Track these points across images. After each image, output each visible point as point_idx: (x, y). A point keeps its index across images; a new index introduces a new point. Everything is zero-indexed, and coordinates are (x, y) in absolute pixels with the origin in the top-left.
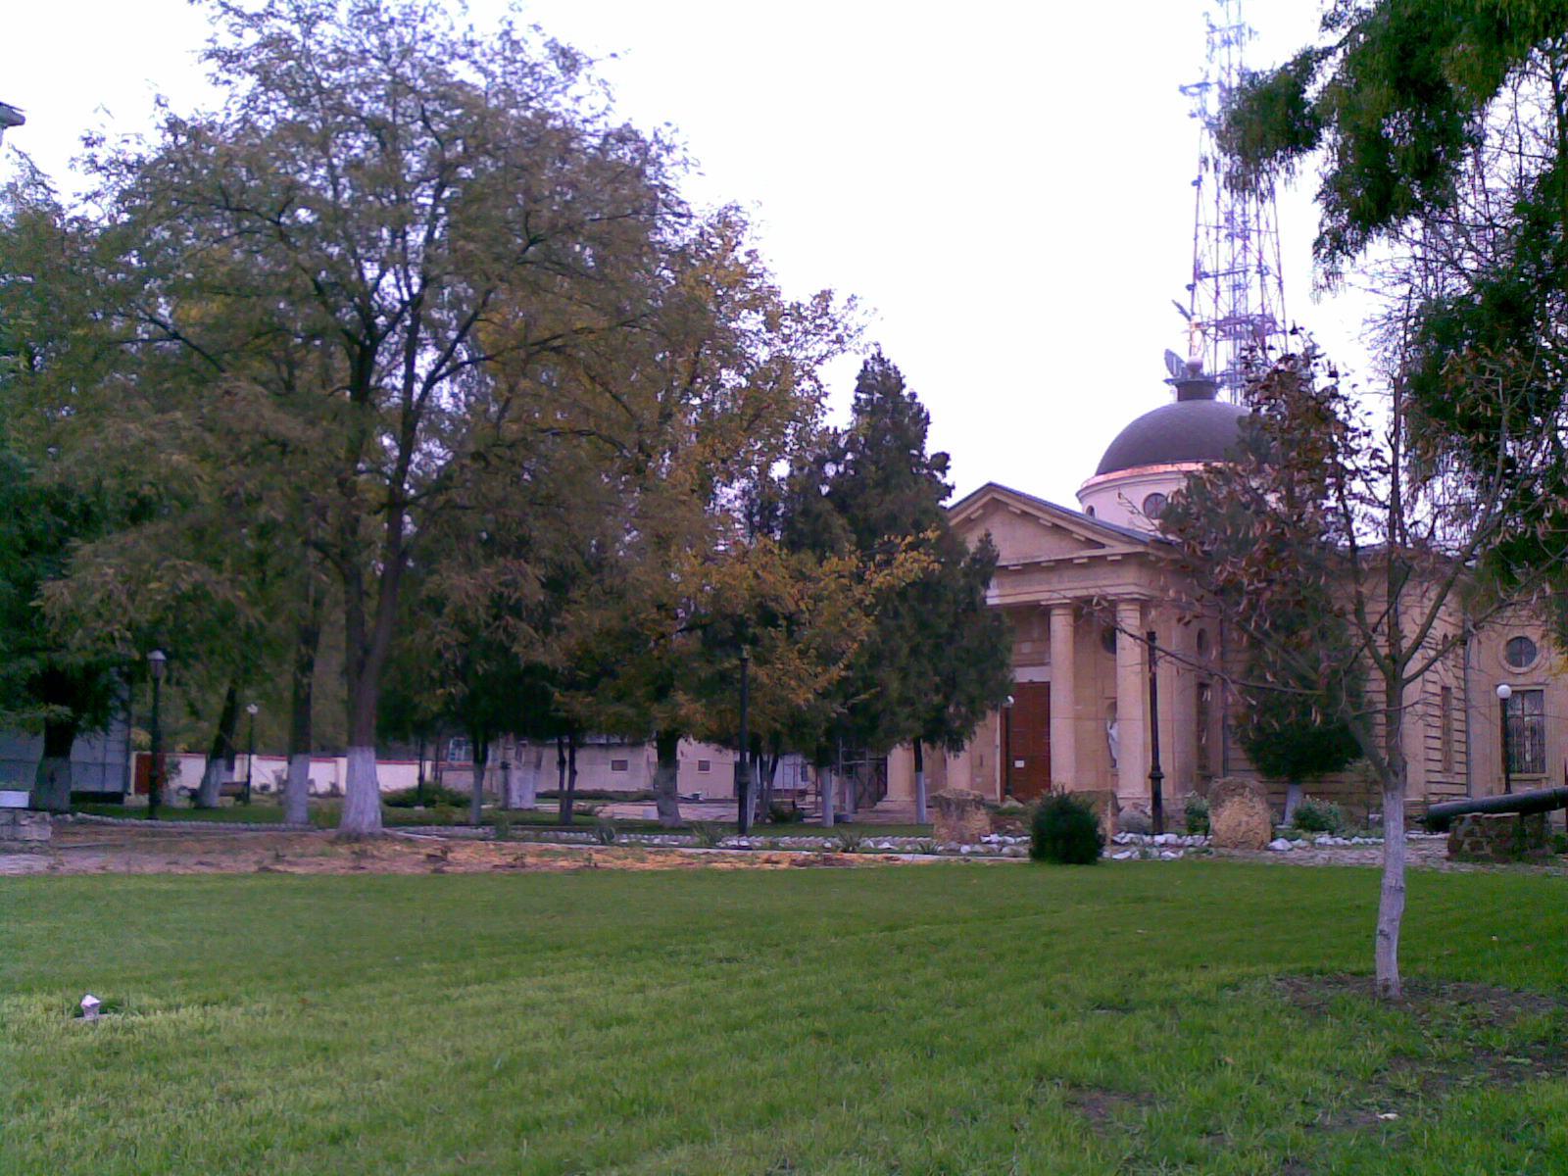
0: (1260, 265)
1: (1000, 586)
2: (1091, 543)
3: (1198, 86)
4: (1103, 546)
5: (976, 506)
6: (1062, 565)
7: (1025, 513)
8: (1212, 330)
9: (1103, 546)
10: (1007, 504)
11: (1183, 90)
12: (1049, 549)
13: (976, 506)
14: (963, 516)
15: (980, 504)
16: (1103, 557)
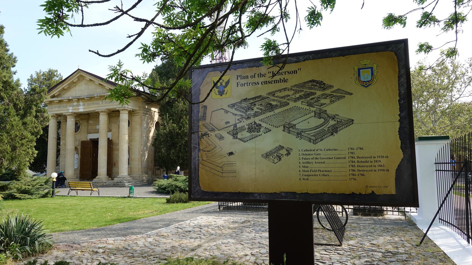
1: (84, 105)
5: (75, 78)
7: (91, 80)
13: (75, 78)
14: (71, 81)
15: (76, 77)
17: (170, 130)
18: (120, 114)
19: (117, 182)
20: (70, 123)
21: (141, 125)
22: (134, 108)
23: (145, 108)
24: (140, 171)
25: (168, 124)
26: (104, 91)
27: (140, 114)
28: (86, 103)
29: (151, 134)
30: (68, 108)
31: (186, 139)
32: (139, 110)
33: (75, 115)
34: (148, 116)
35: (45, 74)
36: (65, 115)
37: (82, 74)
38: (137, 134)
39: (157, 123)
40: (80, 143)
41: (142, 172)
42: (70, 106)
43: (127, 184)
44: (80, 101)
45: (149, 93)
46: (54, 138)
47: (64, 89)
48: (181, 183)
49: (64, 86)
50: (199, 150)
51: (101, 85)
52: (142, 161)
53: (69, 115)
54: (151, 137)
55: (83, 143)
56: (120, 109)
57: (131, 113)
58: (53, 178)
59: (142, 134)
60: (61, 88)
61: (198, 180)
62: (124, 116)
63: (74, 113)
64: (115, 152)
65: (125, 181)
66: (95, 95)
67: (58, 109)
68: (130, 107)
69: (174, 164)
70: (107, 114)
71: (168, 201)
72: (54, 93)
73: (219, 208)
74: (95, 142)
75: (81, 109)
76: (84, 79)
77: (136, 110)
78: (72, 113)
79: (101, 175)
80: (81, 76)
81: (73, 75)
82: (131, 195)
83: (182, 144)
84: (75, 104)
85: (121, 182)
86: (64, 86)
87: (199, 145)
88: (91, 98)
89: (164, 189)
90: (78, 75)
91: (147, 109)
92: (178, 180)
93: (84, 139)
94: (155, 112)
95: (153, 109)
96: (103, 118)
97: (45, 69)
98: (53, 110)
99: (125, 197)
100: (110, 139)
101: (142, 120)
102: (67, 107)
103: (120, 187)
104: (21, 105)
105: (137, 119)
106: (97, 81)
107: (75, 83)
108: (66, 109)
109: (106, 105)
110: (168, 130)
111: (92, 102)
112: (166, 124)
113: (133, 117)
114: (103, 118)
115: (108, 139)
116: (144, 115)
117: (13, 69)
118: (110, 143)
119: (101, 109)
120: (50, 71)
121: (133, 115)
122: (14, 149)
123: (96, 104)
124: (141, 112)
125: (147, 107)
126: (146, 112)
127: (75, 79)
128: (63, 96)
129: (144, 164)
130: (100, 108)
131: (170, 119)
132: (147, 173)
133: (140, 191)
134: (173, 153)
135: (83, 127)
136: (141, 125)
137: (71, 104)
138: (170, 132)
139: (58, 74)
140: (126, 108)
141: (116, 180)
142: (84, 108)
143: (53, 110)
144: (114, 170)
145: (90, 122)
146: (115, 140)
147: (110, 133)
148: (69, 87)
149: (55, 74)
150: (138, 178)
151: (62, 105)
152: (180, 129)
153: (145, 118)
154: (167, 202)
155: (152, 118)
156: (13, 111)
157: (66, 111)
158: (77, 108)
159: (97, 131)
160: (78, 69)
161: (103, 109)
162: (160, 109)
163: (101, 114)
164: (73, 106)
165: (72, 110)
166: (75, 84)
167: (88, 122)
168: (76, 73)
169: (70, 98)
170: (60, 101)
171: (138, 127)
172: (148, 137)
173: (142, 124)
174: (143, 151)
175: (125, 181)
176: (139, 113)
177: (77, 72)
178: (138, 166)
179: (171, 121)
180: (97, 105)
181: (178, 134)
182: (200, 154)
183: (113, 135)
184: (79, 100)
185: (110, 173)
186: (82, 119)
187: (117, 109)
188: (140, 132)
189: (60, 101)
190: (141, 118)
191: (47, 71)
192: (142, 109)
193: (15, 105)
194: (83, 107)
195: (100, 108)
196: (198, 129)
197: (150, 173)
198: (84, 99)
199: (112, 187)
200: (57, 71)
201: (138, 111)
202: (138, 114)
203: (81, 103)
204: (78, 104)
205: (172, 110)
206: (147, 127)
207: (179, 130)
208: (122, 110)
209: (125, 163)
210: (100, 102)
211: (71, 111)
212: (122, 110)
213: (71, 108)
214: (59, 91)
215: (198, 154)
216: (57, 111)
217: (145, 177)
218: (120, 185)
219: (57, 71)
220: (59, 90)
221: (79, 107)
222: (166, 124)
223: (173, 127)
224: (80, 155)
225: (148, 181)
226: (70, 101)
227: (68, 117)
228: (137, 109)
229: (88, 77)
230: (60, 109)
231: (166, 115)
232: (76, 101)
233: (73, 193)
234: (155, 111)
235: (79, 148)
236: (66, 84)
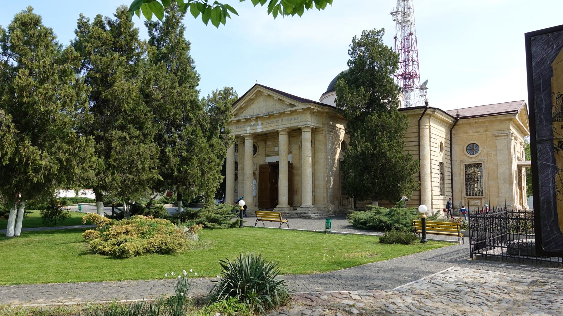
0: (412, 59)
1: (262, 124)
2: (292, 105)
3: (396, 12)
4: (295, 106)
5: (253, 94)
6: (281, 114)
7: (269, 95)
8: (400, 77)
9: (295, 106)
10: (263, 92)
11: (392, 13)
12: (276, 107)
13: (253, 94)
15: (254, 93)
16: (295, 111)
17: (362, 150)
18: (303, 133)
19: (301, 213)
20: (248, 144)
21: (326, 145)
22: (317, 125)
23: (329, 125)
24: (326, 200)
25: (359, 143)
26: (284, 107)
27: (324, 132)
28: (264, 122)
29: (337, 156)
31: (383, 161)
32: (323, 127)
33: (253, 136)
34: (333, 134)
35: (221, 94)
36: (243, 137)
37: (260, 89)
38: (321, 156)
39: (343, 142)
40: (258, 167)
41: (328, 202)
43: (312, 216)
44: (258, 120)
45: (335, 106)
47: (241, 108)
48: (386, 217)
49: (242, 104)
50: (555, 170)
51: (281, 100)
52: (327, 189)
53: (247, 136)
54: (336, 160)
55: (261, 167)
57: (314, 131)
58: (241, 207)
59: (327, 156)
60: (238, 107)
61: (556, 221)
62: (307, 135)
63: (253, 134)
64: (296, 178)
65: (310, 212)
67: (235, 130)
68: (313, 124)
69: (368, 192)
70: (286, 133)
71: (382, 241)
73: (472, 257)
74: (275, 167)
75: (260, 129)
76: (261, 95)
77: (320, 128)
78: (250, 133)
79: (282, 204)
80: (259, 91)
82: (328, 230)
83: (378, 168)
84: (253, 123)
85: (305, 213)
86: (242, 104)
87: (554, 161)
88: (270, 116)
89: (365, 223)
90: (255, 91)
91: (332, 126)
92: (381, 213)
93: (262, 163)
94: (340, 128)
95: (338, 126)
96: (283, 139)
97: (221, 88)
99: (321, 232)
100: (290, 162)
101: (326, 140)
102: (244, 127)
103: (305, 218)
104: (208, 126)
105: (320, 138)
106: (276, 96)
107: (253, 100)
109: (286, 123)
110: (359, 150)
111: (271, 120)
112: (357, 143)
113: (315, 136)
114: (283, 139)
115: (289, 162)
116: (330, 133)
117: (197, 88)
118: (291, 166)
119: (281, 128)
120: (225, 89)
121: (316, 133)
122: (203, 173)
123: (275, 122)
124: (326, 129)
125: (331, 123)
126: (331, 130)
127: (252, 96)
128: (241, 115)
129: (330, 192)
130: (280, 127)
131: (362, 137)
132: (333, 203)
133: (337, 224)
134: (367, 179)
135: (261, 150)
136: (326, 145)
137: (248, 124)
138: (363, 153)
139: (234, 91)
140: (309, 126)
141: (299, 210)
142: (262, 128)
144: (296, 198)
145: (268, 143)
146: (296, 164)
147: (290, 155)
148: (247, 105)
149: (231, 92)
150: (323, 209)
151: (240, 126)
152: (375, 149)
153: (330, 137)
154: (380, 242)
155: (337, 136)
156: (200, 132)
157: (244, 132)
158: (254, 127)
159: (277, 154)
160: (256, 84)
162: (347, 125)
163: (280, 133)
164: (251, 126)
167: (266, 143)
168: (254, 88)
169: (248, 117)
170: (238, 121)
171: (322, 147)
172: (333, 160)
173: (327, 144)
174: (329, 177)
175: (310, 212)
176: (322, 131)
178: (323, 194)
179: (364, 139)
180: (277, 124)
181: (373, 155)
182: (557, 176)
183: (293, 158)
184: (257, 118)
185: (291, 202)
186: (259, 141)
187: (299, 127)
188: (324, 153)
190: (325, 136)
191: (223, 89)
192: (326, 126)
193: (202, 126)
194: (261, 126)
195: (280, 127)
196: (552, 135)
197: (336, 202)
198: (262, 117)
199: (296, 218)
200: (232, 89)
201: (321, 129)
202: (322, 132)
203: (259, 123)
205: (363, 125)
206: (332, 147)
207: (374, 150)
208: (305, 128)
209: (309, 191)
210: (280, 120)
211: (248, 132)
212: (305, 128)
213: (249, 128)
215: (553, 177)
217: (331, 208)
218: (304, 216)
219: (232, 89)
220: (236, 108)
221: (257, 127)
222: (357, 143)
223: (366, 146)
224: (258, 180)
225: (334, 212)
226: (248, 120)
227: (246, 138)
228: (321, 126)
229: (266, 92)
231: (358, 132)
232: (254, 120)
233: (260, 224)
234: (341, 128)
235: (257, 172)
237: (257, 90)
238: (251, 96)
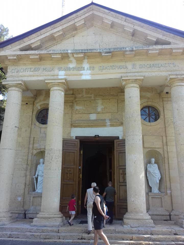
1: (92, 68)
4: (169, 43)
5: (80, 19)
9: (169, 43)
15: (83, 17)
30: (56, 72)
42: (60, 69)
46: (16, 127)
56: (179, 77)
60: (48, 34)
66: (127, 49)
67: (31, 73)
72: (32, 41)
81: (78, 13)
84: (71, 66)
90: (87, 15)
98: (21, 74)
102: (53, 70)
108: (52, 73)
111: (111, 64)
127: (79, 21)
137: (63, 66)
143: (21, 74)
145: (77, 107)
158: (75, 72)
161: (139, 76)
164: (68, 69)
165: (65, 75)
166: (74, 33)
168: (85, 10)
177: (87, 8)
189: (41, 59)
204: (79, 66)
214: (41, 40)
216: (31, 76)
221: (81, 72)
226: (65, 57)
230: (37, 72)
236: (60, 28)
237: (91, 13)
238: (76, 20)
